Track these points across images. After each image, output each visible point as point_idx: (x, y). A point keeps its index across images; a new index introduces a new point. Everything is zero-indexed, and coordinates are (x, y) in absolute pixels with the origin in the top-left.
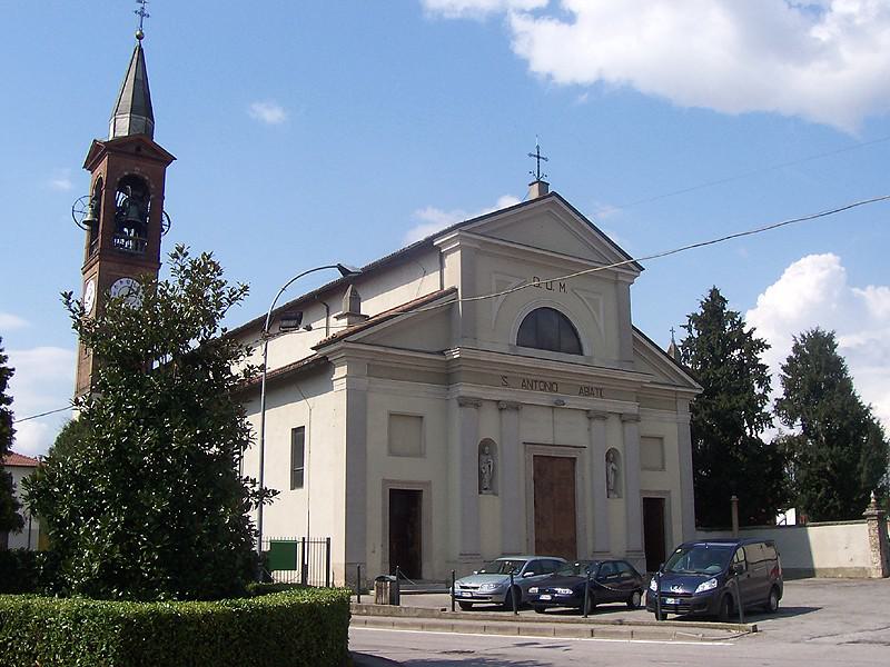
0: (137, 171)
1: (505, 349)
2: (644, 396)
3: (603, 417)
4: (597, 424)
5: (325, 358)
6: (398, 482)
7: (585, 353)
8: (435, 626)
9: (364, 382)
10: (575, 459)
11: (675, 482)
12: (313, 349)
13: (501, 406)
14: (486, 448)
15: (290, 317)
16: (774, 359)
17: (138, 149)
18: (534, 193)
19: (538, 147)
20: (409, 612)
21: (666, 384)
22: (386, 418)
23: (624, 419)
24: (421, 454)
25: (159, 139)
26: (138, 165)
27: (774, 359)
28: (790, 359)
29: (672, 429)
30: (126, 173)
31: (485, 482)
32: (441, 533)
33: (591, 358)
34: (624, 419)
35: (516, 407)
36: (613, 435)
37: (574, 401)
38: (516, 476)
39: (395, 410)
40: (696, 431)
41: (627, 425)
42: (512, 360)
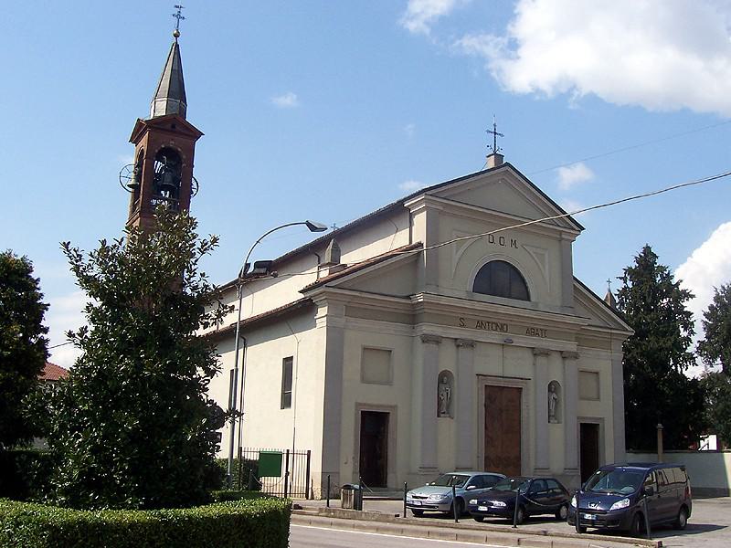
0: (172, 144)
2: (582, 336)
3: (546, 353)
4: (541, 360)
5: (310, 300)
6: (369, 405)
7: (533, 299)
8: (387, 530)
9: (342, 321)
10: (521, 388)
11: (608, 410)
12: (300, 292)
14: (444, 378)
16: (698, 307)
17: (173, 126)
18: (491, 163)
19: (495, 125)
20: (368, 517)
21: (601, 327)
22: (360, 352)
23: (564, 356)
24: (389, 383)
25: (191, 118)
27: (698, 307)
28: (711, 307)
29: (607, 365)
31: (443, 408)
32: (404, 448)
33: (537, 304)
34: (564, 356)
35: (471, 344)
36: (555, 369)
37: (522, 341)
38: (470, 402)
40: (627, 370)
41: (567, 362)
42: (468, 304)
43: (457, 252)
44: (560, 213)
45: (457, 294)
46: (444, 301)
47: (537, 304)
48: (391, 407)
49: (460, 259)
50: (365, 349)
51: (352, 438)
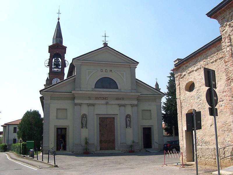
0: (58, 52)
1: (90, 89)
3: (124, 106)
10: (114, 118)
13: (89, 105)
17: (58, 46)
18: (103, 46)
19: (105, 34)
23: (132, 106)
25: (64, 44)
26: (58, 51)
30: (55, 53)
33: (120, 89)
34: (132, 106)
35: (93, 105)
36: (129, 111)
39: (59, 107)
42: (93, 92)
43: (88, 76)
45: (88, 89)
46: (84, 92)
47: (120, 89)
49: (89, 78)
50: (57, 109)
51: (53, 136)
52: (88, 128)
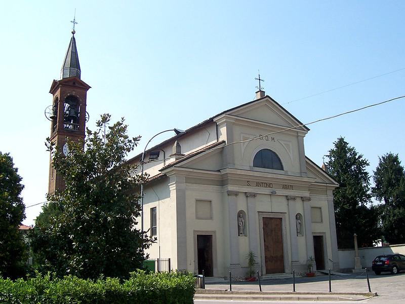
1: (248, 168)
2: (311, 188)
3: (294, 198)
4: (291, 202)
5: (165, 175)
6: (203, 232)
7: (285, 168)
8: (223, 298)
9: (184, 186)
11: (327, 228)
12: (159, 171)
13: (247, 195)
14: (241, 215)
15: (153, 154)
16: (371, 169)
17: (74, 83)
19: (259, 76)
20: (210, 292)
21: (321, 183)
22: (194, 202)
23: (303, 199)
24: (211, 218)
25: (84, 78)
26: (74, 91)
27: (371, 169)
28: (378, 169)
29: (325, 203)
30: (69, 95)
31: (241, 231)
32: (220, 256)
33: (287, 172)
34: (303, 199)
35: (254, 195)
36: (298, 207)
37: (280, 192)
38: (255, 227)
39: (199, 198)
40: (336, 204)
41: (305, 203)
42: (251, 173)
44: (298, 124)
45: (245, 168)
46: (239, 172)
48: (213, 231)
52: (248, 234)
